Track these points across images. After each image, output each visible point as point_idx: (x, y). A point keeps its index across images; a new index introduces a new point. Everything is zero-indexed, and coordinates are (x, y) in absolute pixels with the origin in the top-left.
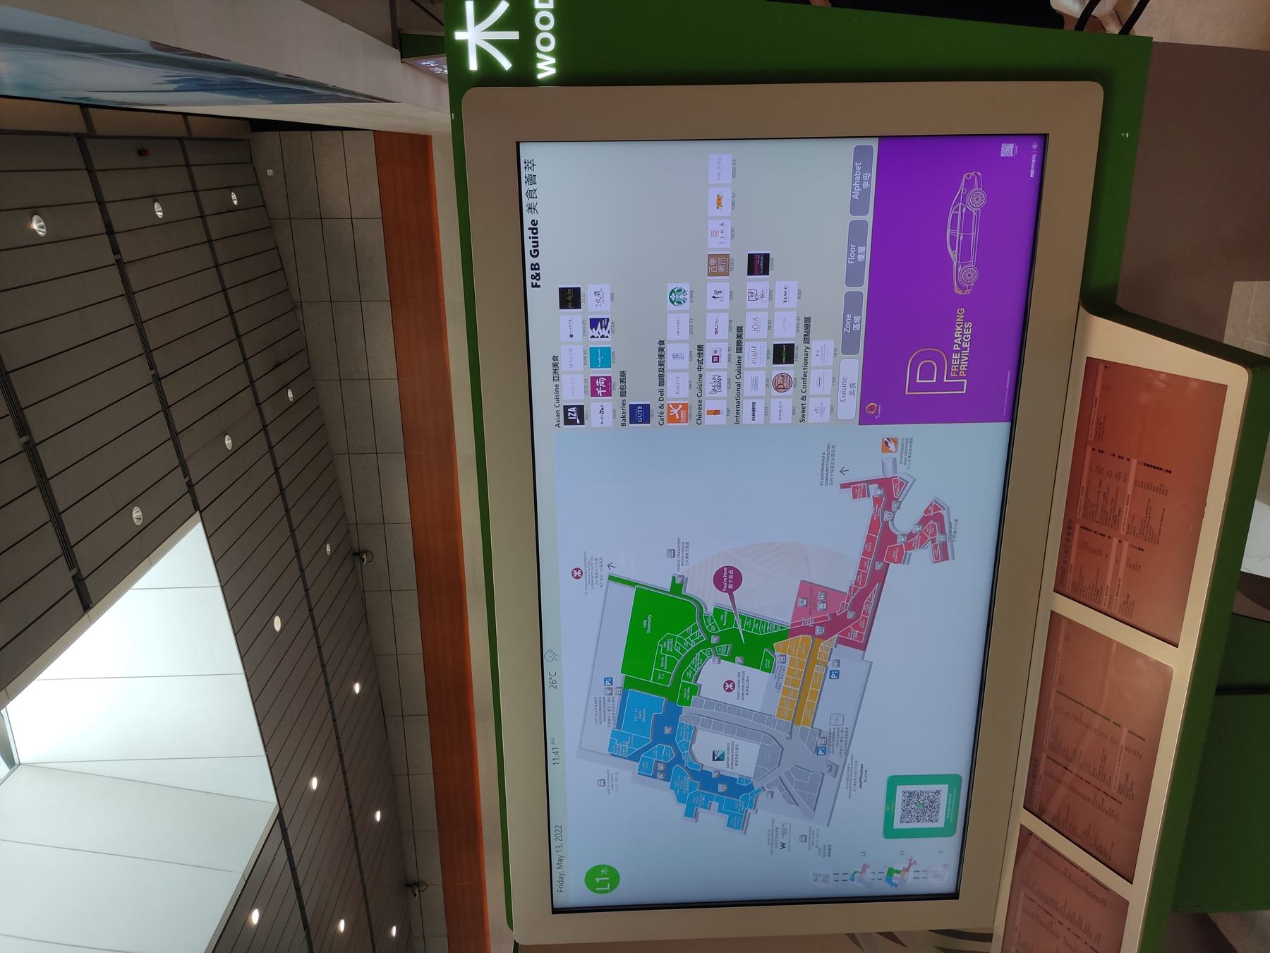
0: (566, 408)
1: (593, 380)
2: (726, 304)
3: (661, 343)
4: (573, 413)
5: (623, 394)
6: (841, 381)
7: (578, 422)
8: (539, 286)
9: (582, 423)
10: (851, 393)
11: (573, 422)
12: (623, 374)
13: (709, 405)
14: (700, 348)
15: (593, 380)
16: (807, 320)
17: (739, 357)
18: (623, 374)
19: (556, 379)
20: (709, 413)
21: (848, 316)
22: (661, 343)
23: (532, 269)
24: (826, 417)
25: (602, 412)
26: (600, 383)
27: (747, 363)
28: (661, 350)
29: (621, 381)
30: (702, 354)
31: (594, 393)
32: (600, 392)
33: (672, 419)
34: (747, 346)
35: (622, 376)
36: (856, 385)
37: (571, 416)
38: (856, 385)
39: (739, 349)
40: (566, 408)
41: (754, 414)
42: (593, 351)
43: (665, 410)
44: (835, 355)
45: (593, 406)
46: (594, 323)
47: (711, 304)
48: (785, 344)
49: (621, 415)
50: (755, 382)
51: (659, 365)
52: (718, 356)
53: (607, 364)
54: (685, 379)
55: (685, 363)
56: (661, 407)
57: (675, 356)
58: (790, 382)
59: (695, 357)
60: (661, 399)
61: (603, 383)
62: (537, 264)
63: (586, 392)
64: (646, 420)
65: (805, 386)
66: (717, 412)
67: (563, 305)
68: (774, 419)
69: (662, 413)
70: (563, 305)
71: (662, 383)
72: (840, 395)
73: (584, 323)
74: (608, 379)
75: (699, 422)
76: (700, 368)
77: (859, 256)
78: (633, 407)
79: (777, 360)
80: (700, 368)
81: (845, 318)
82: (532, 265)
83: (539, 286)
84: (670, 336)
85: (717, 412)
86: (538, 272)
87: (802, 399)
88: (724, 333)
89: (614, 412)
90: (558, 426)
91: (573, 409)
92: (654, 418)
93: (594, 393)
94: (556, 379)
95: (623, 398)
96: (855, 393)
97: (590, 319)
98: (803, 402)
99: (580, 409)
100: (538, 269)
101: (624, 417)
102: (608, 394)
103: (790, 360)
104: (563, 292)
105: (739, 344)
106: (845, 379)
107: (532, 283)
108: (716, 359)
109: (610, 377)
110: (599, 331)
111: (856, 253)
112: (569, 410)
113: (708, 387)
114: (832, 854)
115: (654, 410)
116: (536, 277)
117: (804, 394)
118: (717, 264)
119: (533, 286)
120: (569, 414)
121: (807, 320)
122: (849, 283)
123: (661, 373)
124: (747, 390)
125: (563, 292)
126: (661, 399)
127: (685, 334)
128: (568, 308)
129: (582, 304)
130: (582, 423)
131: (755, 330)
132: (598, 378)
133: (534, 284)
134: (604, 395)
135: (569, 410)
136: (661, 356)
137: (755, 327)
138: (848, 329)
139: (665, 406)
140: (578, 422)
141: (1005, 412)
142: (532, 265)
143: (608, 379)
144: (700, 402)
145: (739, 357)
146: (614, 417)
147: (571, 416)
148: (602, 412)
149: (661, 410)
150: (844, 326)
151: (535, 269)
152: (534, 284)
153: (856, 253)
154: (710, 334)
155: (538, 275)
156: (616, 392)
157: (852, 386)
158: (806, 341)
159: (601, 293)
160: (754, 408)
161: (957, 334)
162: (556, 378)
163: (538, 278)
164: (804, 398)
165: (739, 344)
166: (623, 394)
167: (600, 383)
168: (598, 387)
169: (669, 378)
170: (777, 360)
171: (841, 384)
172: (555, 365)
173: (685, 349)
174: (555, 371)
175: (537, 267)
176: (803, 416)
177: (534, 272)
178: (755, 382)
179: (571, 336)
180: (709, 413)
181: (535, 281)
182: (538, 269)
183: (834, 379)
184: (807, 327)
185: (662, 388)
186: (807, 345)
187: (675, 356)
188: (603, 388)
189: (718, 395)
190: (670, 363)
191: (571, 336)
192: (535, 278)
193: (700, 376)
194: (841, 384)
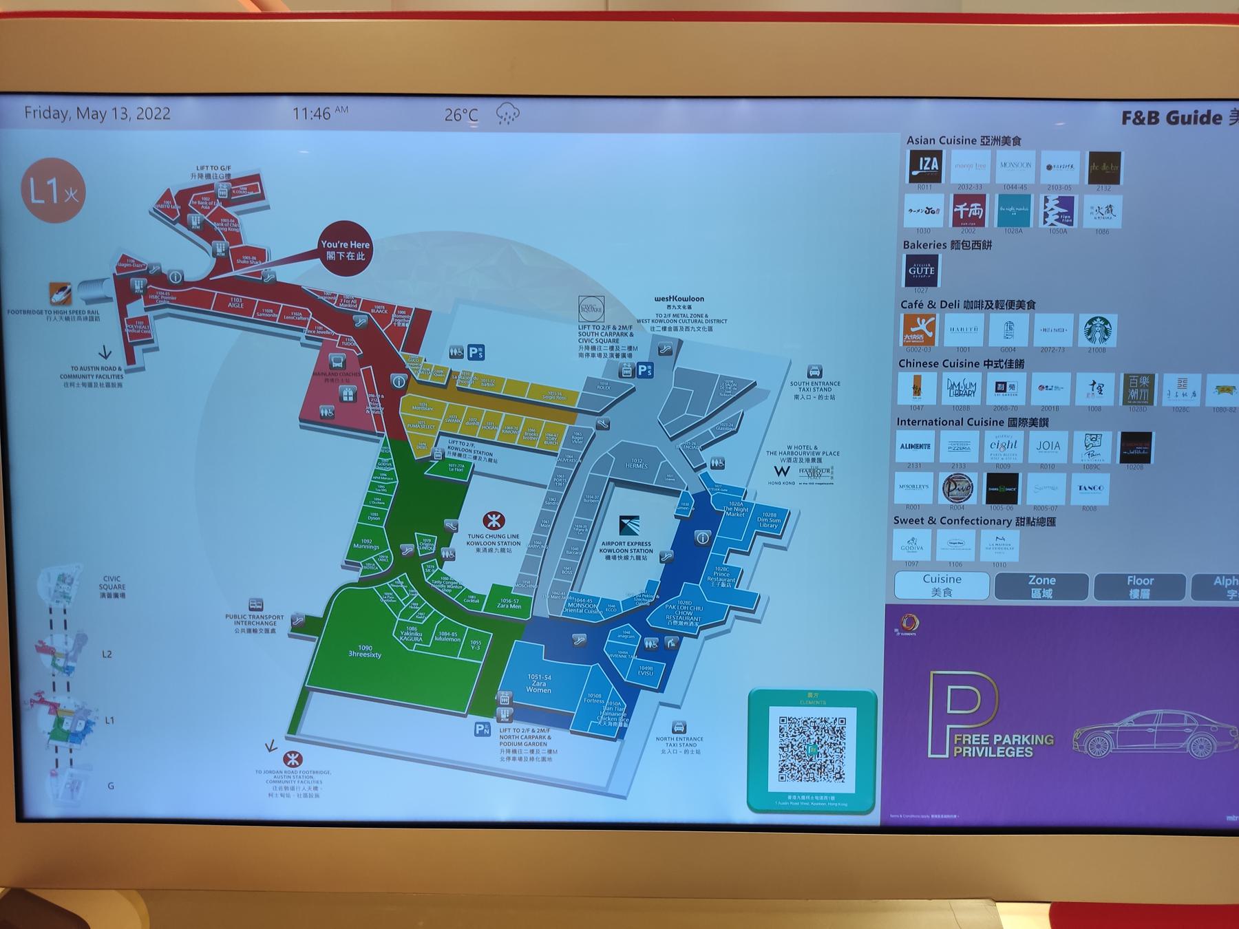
0: (938, 154)
1: (981, 199)
2: (1082, 400)
3: (1032, 305)
4: (930, 165)
5: (955, 245)
6: (956, 575)
7: (915, 173)
8: (1124, 123)
9: (913, 179)
10: (936, 591)
11: (914, 165)
12: (987, 245)
13: (929, 378)
14: (1020, 364)
15: (981, 199)
16: (1052, 522)
17: (1001, 423)
18: (987, 245)
19: (985, 141)
20: (917, 379)
21: (1053, 581)
22: (1032, 305)
23: (1150, 113)
24: (899, 555)
25: (929, 211)
26: (975, 209)
27: (992, 435)
28: (1021, 305)
29: (976, 242)
30: (1011, 367)
31: (959, 199)
32: (961, 208)
33: (910, 322)
34: (1017, 434)
35: (984, 244)
36: (948, 597)
37: (924, 162)
38: (948, 597)
39: (1013, 423)
40: (938, 154)
41: (921, 446)
42: (1024, 200)
43: (925, 310)
44: (996, 564)
45: (937, 198)
46: (1067, 203)
47: (1084, 379)
48: (1017, 490)
49: (922, 242)
50: (962, 447)
51: (997, 301)
52: (1005, 391)
53: (1005, 220)
54: (975, 341)
55: (998, 340)
56: (931, 305)
57: (1010, 325)
58: (959, 500)
59: (1006, 357)
60: (944, 304)
61: (975, 214)
62: (1157, 121)
63: (961, 186)
64: (911, 281)
65: (951, 522)
66: (917, 390)
67: (1096, 158)
68: (901, 478)
69: (921, 305)
70: (1096, 158)
71: (970, 305)
72: (934, 575)
73: (1068, 187)
74: (979, 222)
75: (903, 363)
76: (988, 363)
77: (1137, 591)
78: (933, 260)
79: (993, 479)
80: (988, 363)
81: (1050, 576)
82: (1157, 114)
83: (1124, 123)
84: (1042, 319)
85: (917, 390)
86: (1146, 121)
87: (931, 518)
88: (1040, 399)
89: (927, 230)
90: (910, 140)
91: (935, 166)
92: (915, 294)
93: (959, 199)
94: (985, 141)
95: (949, 245)
96: (937, 597)
97: (1073, 197)
98: (925, 521)
99: (935, 177)
100: (1150, 123)
101: (919, 246)
102: (957, 221)
103: (992, 498)
104: (1114, 158)
105: (1023, 422)
106: (958, 580)
107: (1130, 112)
108: (1001, 387)
109: (983, 225)
110: (1055, 210)
111: (1143, 587)
112: (935, 159)
113: (956, 376)
114: (106, 600)
115: (925, 293)
116: (1139, 120)
117: (938, 521)
118: (1140, 387)
119: (1125, 113)
120: (928, 159)
121: (1052, 522)
122: (1101, 579)
123: (985, 304)
124: (949, 435)
125: (1114, 158)
126: (944, 304)
127: (1041, 341)
128: (1091, 164)
129: (1096, 186)
130: (913, 179)
131: (1041, 445)
132: (983, 206)
133: (1128, 115)
134: (956, 215)
135: (935, 159)
136: (1011, 305)
137: (1046, 445)
138: (1034, 581)
139: (932, 311)
140: (915, 173)
141: (898, 817)
142: (1157, 114)
143: (979, 222)
144: (936, 364)
145: (1001, 423)
146: (920, 230)
147: (924, 162)
148: (929, 211)
149: (926, 304)
150: (1038, 575)
151: (1150, 118)
152: (1128, 115)
153: (1143, 587)
154: (1039, 378)
155: (1142, 122)
156: (961, 234)
157: (948, 592)
158: (1021, 522)
159: (1109, 215)
160: (921, 446)
161: (1016, 738)
162: (986, 141)
163: (1137, 121)
164: (932, 521)
165: (1023, 422)
166: (955, 245)
167: (975, 209)
168: (968, 206)
169: (977, 318)
170: (993, 479)
171: (951, 575)
172: (1006, 141)
173: (1019, 340)
174: (996, 140)
175: (1153, 120)
176: (904, 521)
177: (1145, 115)
178: (962, 447)
179: (1049, 167)
180: (917, 379)
181: (1133, 116)
182: (1150, 123)
183: (959, 564)
184: (1042, 522)
185: (962, 304)
186: (1014, 522)
187: (1010, 325)
188: (966, 213)
189: (945, 392)
190: (999, 318)
191: (1049, 167)
192: (1137, 117)
193: (977, 364)
194: (951, 575)
